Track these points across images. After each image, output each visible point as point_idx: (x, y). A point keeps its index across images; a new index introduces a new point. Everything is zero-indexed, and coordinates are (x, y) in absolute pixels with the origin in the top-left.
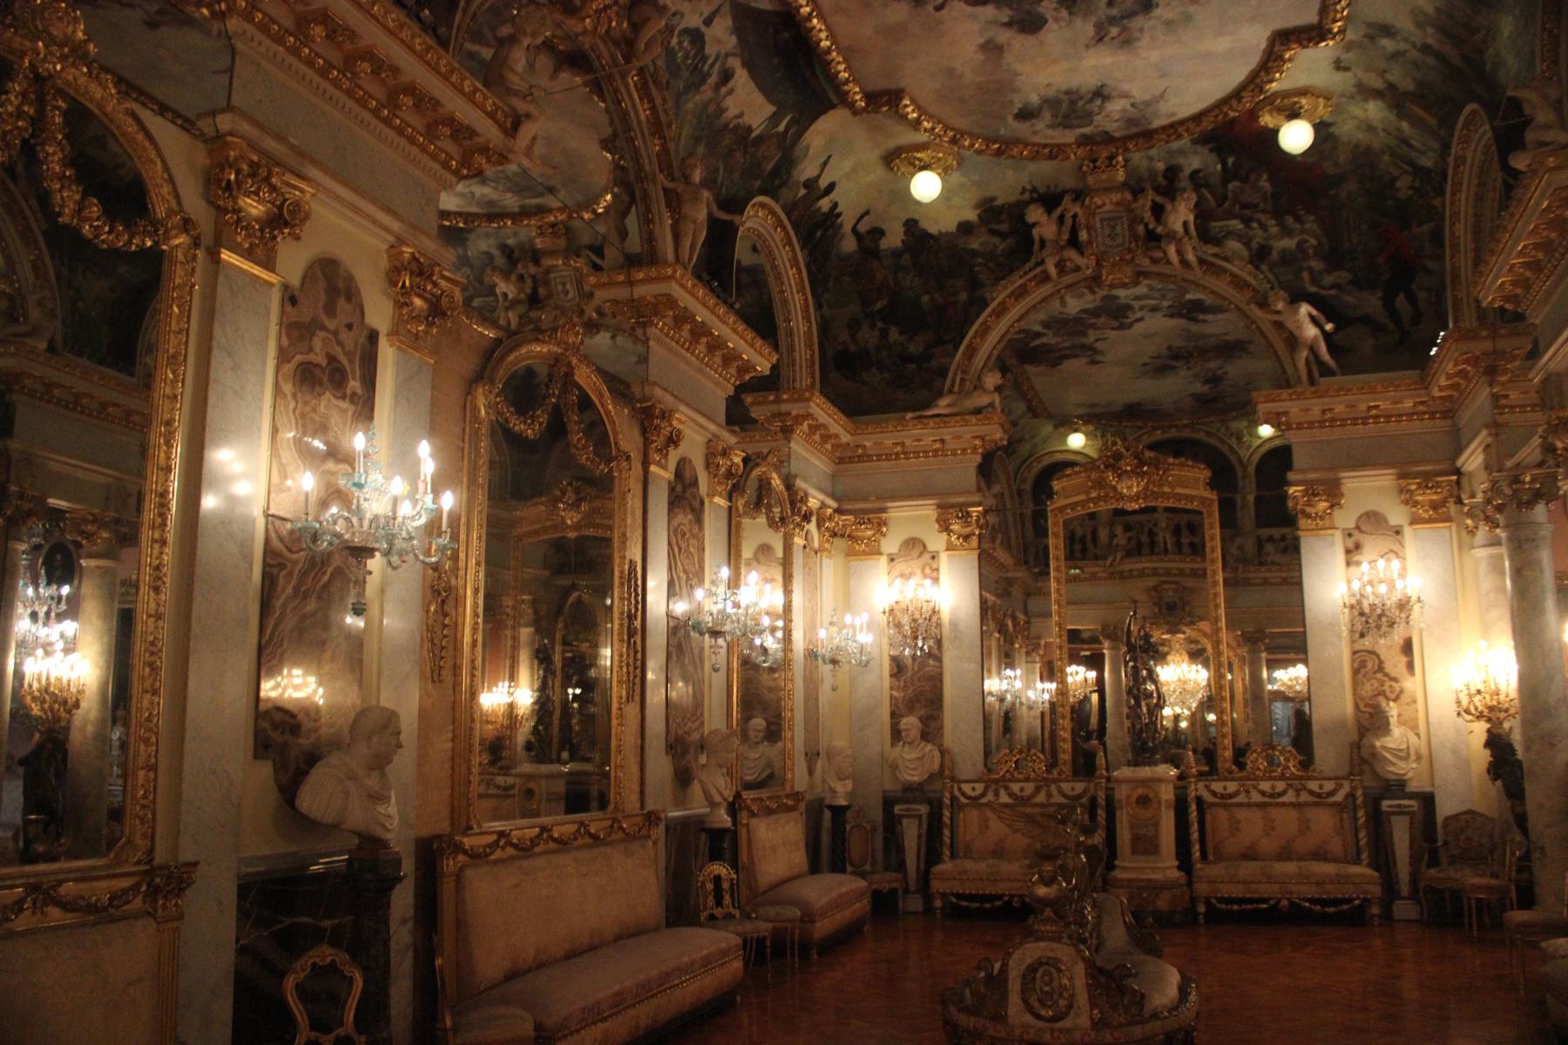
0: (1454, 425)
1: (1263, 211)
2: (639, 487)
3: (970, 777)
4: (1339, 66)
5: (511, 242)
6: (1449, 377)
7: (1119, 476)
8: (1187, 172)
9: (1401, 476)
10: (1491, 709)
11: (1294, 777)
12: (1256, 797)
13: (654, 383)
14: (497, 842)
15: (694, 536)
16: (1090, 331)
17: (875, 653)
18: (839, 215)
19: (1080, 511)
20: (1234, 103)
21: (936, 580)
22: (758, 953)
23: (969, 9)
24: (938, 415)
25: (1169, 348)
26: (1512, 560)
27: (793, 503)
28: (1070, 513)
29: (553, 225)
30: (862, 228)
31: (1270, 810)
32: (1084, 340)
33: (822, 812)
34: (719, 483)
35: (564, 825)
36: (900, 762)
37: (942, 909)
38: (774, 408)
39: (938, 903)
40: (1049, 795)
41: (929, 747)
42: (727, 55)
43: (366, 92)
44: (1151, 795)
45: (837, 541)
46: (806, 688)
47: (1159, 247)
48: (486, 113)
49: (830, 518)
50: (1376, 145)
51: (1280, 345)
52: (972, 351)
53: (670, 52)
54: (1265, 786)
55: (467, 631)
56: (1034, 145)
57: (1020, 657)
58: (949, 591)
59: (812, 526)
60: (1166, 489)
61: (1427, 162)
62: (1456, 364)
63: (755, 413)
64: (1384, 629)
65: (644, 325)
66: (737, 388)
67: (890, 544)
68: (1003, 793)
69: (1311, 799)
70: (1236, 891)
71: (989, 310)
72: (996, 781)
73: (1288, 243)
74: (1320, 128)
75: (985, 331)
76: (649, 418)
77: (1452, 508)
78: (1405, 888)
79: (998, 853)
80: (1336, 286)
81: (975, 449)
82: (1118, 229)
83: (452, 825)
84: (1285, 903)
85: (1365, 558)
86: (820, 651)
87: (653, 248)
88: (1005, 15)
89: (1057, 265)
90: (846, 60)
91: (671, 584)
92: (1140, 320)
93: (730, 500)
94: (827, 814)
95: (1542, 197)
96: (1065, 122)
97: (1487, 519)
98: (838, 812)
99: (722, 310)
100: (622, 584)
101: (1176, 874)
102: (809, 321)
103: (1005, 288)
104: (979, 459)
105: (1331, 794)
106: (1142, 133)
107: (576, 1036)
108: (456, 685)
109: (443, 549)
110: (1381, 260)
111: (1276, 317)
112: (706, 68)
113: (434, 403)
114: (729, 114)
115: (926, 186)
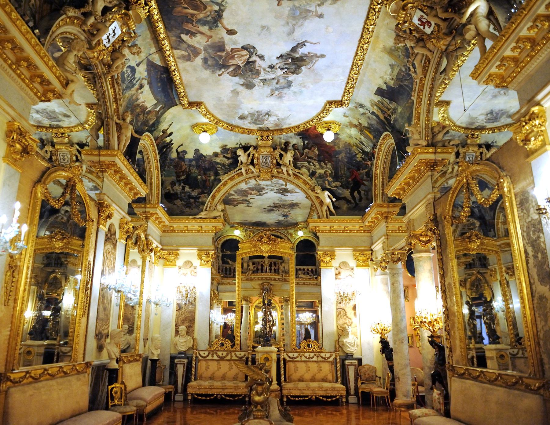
1: (315, 160)
3: (204, 349)
4: (345, 116)
6: (372, 218)
8: (291, 144)
9: (354, 250)
12: (304, 359)
14: (25, 376)
17: (172, 302)
18: (173, 144)
19: (248, 255)
20: (311, 123)
24: (201, 218)
25: (274, 203)
27: (147, 245)
30: (179, 150)
31: (308, 363)
32: (248, 199)
36: (178, 343)
40: (232, 356)
41: (189, 337)
42: (143, 79)
43: (7, 56)
45: (161, 260)
49: (159, 252)
50: (352, 143)
52: (214, 197)
53: (123, 73)
54: (307, 355)
56: (243, 128)
59: (152, 254)
60: (277, 250)
62: (375, 215)
63: (136, 211)
64: (348, 301)
67: (180, 262)
72: (213, 351)
73: (322, 171)
74: (336, 134)
75: (219, 190)
77: (370, 262)
80: (336, 187)
82: (268, 161)
83: (6, 369)
86: (153, 300)
88: (242, 81)
89: (246, 170)
90: (184, 89)
102: (159, 180)
110: (350, 180)
111: (317, 195)
112: (135, 82)
114: (139, 101)
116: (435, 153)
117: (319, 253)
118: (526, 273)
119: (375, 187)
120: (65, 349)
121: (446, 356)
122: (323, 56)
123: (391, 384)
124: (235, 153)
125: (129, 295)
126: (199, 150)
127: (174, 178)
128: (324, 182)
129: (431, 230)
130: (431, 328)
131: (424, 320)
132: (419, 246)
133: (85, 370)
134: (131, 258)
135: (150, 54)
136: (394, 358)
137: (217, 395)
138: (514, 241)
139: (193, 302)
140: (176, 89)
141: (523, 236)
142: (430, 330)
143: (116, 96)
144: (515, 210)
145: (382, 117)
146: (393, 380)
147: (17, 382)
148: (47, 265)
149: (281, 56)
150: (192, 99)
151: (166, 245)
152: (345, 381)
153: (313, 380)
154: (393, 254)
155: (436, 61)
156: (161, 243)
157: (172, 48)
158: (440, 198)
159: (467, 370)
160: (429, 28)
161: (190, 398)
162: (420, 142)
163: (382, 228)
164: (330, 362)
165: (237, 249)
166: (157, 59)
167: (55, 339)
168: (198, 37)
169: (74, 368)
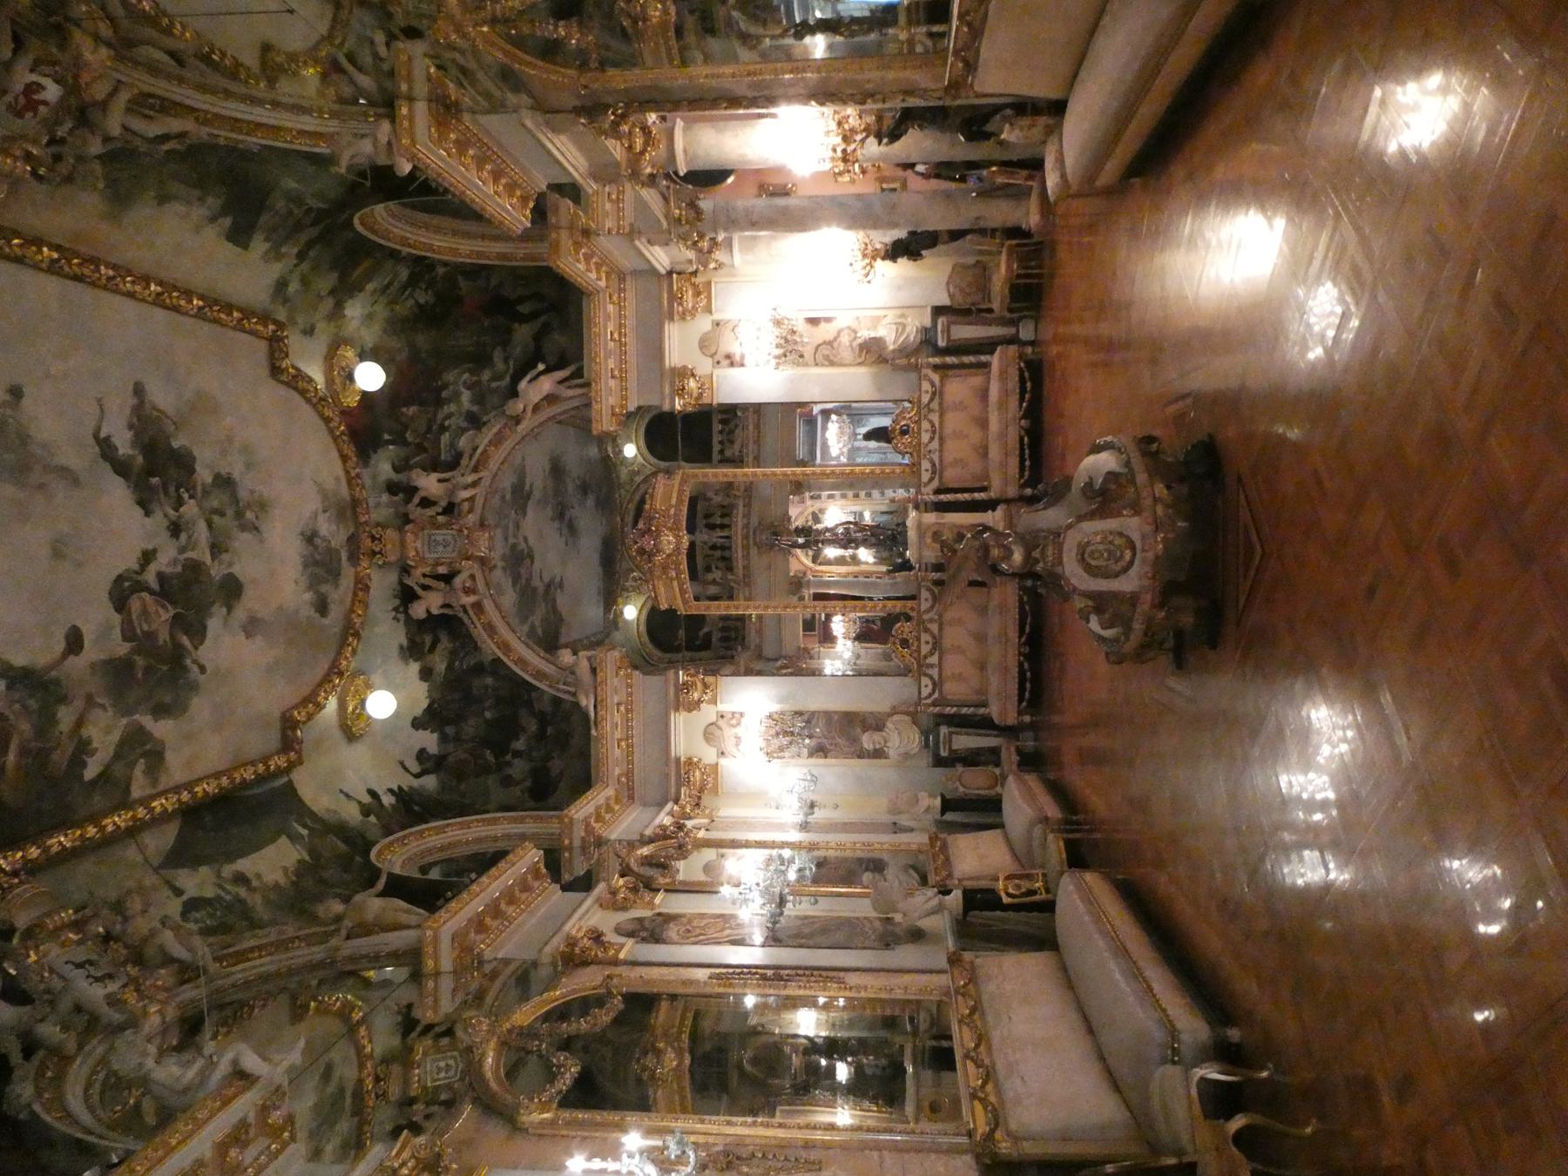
1: (435, 415)
4: (309, 331)
9: (671, 319)
10: (865, 256)
11: (919, 413)
12: (935, 445)
15: (690, 922)
19: (688, 585)
21: (742, 715)
23: (208, 642)
25: (553, 519)
26: (743, 229)
27: (666, 837)
28: (690, 595)
30: (415, 768)
32: (541, 590)
33: (947, 823)
34: (642, 898)
36: (902, 750)
38: (577, 852)
40: (931, 620)
41: (889, 725)
42: (219, 876)
45: (704, 802)
46: (835, 831)
48: (220, 1109)
49: (683, 808)
52: (540, 675)
54: (925, 437)
55: (770, 1132)
56: (353, 603)
57: (814, 664)
58: (751, 700)
59: (689, 824)
60: (672, 511)
61: (404, 274)
65: (481, 963)
67: (708, 755)
71: (505, 659)
72: (920, 666)
73: (466, 396)
74: (363, 357)
75: (521, 662)
76: (572, 959)
77: (699, 280)
78: (1013, 331)
80: (506, 360)
81: (629, 676)
82: (439, 538)
85: (735, 349)
86: (800, 818)
88: (219, 611)
90: (245, 765)
94: (949, 816)
96: (335, 574)
97: (710, 252)
98: (947, 805)
99: (474, 887)
100: (731, 985)
105: (933, 385)
106: (349, 510)
108: (827, 1146)
111: (530, 408)
112: (228, 897)
114: (282, 881)
115: (381, 705)
116: (411, 99)
117: (678, 407)
120: (923, 1021)
122: (139, 390)
123: (993, 236)
125: (792, 876)
126: (415, 719)
128: (495, 390)
129: (616, 124)
130: (859, 137)
131: (839, 154)
132: (656, 154)
134: (701, 877)
135: (146, 859)
136: (931, 229)
140: (245, 784)
142: (863, 141)
143: (272, 944)
145: (313, 232)
146: (982, 232)
148: (723, 1087)
149: (145, 505)
150: (273, 739)
151: (667, 791)
152: (988, 346)
153: (983, 423)
154: (679, 220)
155: (146, 77)
156: (661, 805)
157: (125, 804)
159: (956, 53)
160: (44, 88)
161: (1027, 719)
162: (383, 139)
163: (607, 244)
165: (671, 612)
166: (160, 841)
167: (902, 1047)
168: (92, 731)
169: (962, 992)
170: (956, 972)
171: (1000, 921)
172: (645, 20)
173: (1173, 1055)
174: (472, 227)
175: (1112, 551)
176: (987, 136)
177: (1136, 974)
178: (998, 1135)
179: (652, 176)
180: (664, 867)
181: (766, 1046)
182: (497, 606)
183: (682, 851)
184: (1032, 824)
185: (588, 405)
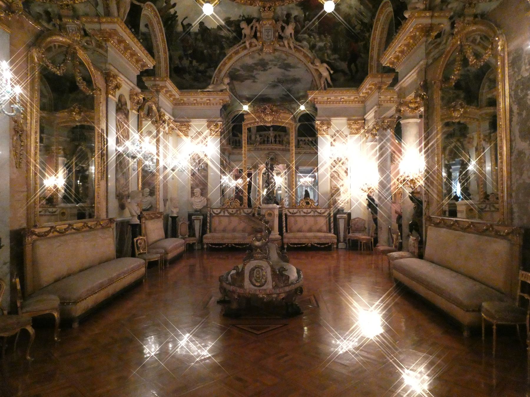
0: (365, 105)
2: (105, 102)
5: (50, 10)
7: (265, 115)
8: (293, 16)
9: (348, 120)
12: (302, 214)
13: (110, 64)
14: (50, 230)
16: (254, 71)
18: (177, 16)
22: (151, 265)
24: (208, 91)
25: (278, 79)
27: (160, 116)
28: (249, 126)
29: (67, 5)
30: (185, 23)
35: (78, 224)
37: (207, 248)
38: (153, 83)
39: (205, 246)
44: (272, 213)
47: (283, 41)
51: (316, 77)
52: (220, 71)
54: (305, 210)
59: (166, 125)
60: (279, 120)
61: (366, 21)
62: (370, 85)
65: (105, 41)
66: (141, 72)
67: (192, 132)
68: (226, 212)
69: (318, 214)
70: (296, 241)
71: (227, 57)
72: (224, 208)
73: (321, 44)
75: (225, 64)
76: (108, 77)
78: (342, 241)
79: (234, 230)
80: (335, 59)
82: (270, 33)
84: (310, 244)
87: (109, 11)
91: (117, 138)
92: (270, 68)
93: (138, 112)
94: (170, 219)
95: (411, 27)
98: (174, 219)
99: (136, 40)
101: (278, 236)
103: (232, 50)
104: (221, 107)
105: (323, 213)
107: (85, 301)
108: (28, 171)
109: (17, 110)
113: (12, 52)
116: (432, 17)
118: (508, 131)
119: (372, 58)
121: (424, 208)
124: (239, 26)
125: (147, 163)
127: (180, 52)
128: (323, 54)
129: (420, 96)
130: (412, 185)
132: (408, 112)
133: (108, 226)
137: (228, 244)
138: (501, 100)
139: (206, 168)
141: (510, 95)
142: (411, 187)
144: (506, 69)
146: (376, 229)
147: (42, 236)
152: (337, 232)
156: (173, 116)
158: (431, 64)
159: (442, 219)
162: (418, 6)
164: (324, 216)
165: (243, 120)
170: (107, 221)
171: (128, 237)
172: (454, 111)
173: (64, 302)
174: (383, 46)
175: (259, 279)
176: (411, 231)
177: (102, 287)
178: (34, 237)
179: (400, 111)
180: (148, 115)
181: (86, 155)
182: (245, 55)
183: (155, 123)
184: (163, 248)
185: (317, 89)
